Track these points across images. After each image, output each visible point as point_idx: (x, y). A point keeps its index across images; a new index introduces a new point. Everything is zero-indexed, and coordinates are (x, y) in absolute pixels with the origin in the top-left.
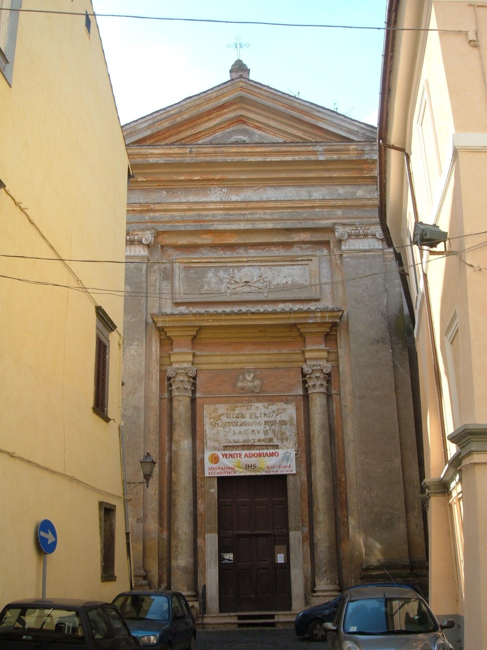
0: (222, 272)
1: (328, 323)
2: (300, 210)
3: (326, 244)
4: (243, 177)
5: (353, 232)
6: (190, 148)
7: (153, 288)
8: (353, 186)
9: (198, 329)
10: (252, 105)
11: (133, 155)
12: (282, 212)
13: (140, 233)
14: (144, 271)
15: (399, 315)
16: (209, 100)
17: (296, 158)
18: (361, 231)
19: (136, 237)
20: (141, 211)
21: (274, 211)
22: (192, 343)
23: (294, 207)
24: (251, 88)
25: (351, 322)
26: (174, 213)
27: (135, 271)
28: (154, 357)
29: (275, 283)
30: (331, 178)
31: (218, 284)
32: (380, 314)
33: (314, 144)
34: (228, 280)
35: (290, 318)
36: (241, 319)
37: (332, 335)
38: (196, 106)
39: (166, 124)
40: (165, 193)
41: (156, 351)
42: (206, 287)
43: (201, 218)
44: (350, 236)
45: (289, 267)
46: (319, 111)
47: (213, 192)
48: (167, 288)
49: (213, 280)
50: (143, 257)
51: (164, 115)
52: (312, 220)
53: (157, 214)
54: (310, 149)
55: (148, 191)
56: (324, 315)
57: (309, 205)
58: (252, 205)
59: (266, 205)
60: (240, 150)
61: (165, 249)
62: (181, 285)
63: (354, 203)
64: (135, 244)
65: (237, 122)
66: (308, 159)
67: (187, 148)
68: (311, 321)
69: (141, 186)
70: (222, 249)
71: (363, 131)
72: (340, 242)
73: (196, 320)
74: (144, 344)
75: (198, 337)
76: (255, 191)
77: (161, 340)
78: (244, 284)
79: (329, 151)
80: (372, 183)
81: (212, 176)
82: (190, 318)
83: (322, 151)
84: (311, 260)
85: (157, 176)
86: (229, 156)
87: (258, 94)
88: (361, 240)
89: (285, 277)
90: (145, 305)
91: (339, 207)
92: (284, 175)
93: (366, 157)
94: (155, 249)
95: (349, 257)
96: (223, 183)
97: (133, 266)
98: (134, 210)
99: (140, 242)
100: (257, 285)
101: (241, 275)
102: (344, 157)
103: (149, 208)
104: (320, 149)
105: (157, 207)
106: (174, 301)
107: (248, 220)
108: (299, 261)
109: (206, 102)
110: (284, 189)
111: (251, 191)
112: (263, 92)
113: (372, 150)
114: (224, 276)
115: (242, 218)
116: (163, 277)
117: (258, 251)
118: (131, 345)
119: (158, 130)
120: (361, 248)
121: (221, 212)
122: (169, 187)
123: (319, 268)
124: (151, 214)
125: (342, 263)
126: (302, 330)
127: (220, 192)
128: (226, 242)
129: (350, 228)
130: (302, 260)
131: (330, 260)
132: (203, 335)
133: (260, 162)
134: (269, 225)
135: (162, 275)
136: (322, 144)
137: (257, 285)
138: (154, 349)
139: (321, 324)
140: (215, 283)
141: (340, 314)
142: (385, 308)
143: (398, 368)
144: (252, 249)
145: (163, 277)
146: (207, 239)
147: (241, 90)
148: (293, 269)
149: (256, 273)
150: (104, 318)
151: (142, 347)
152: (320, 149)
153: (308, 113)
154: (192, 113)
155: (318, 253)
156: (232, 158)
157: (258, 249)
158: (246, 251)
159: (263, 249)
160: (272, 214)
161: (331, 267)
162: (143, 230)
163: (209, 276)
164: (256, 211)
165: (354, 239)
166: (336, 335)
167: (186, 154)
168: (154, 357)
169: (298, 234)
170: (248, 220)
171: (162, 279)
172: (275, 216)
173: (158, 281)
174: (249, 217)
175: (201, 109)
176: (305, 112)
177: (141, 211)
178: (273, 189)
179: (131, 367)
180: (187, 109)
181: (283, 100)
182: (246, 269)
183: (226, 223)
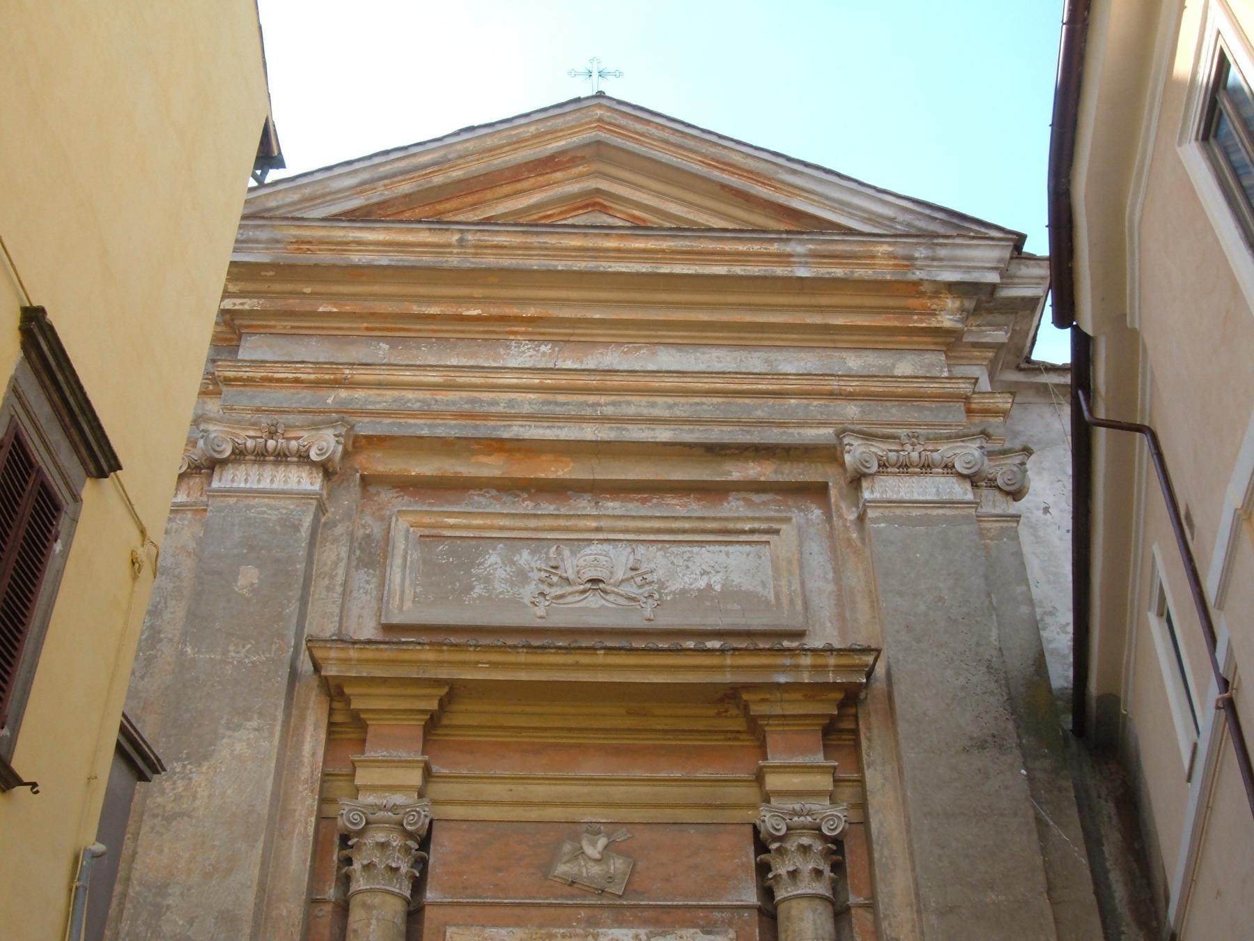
0: (525, 554)
1: (834, 686)
2: (747, 401)
3: (818, 492)
4: (597, 316)
5: (893, 456)
6: (462, 231)
7: (327, 581)
8: (883, 354)
9: (444, 691)
10: (621, 166)
11: (310, 243)
12: (697, 404)
13: (305, 434)
14: (304, 532)
15: (1036, 678)
16: (518, 143)
17: (738, 270)
18: (915, 455)
19: (294, 444)
20: (317, 384)
21: (677, 400)
22: (426, 741)
23: (731, 391)
24: (623, 122)
25: (901, 689)
26: (404, 393)
27: (278, 528)
28: (305, 772)
29: (675, 586)
30: (827, 328)
31: (512, 584)
32: (984, 669)
33: (784, 236)
34: (543, 574)
35: (721, 668)
36: (577, 666)
37: (842, 731)
38: (484, 151)
39: (406, 188)
40: (387, 347)
41: (314, 754)
42: (479, 590)
43: (478, 409)
44: (883, 465)
45: (717, 548)
46: (794, 172)
47: (514, 350)
48: (368, 587)
49: (501, 573)
50: (305, 495)
51: (401, 165)
52: (780, 425)
53: (359, 394)
54: (774, 248)
55: (343, 339)
56: (820, 661)
57: (770, 387)
58: (615, 381)
59: (655, 383)
60: (590, 243)
61: (372, 490)
62: (407, 583)
63: (891, 387)
64: (288, 463)
65: (586, 206)
66: (767, 274)
67: (452, 231)
68: (782, 679)
69: (323, 328)
70: (531, 497)
71: (908, 218)
72: (857, 480)
73: (441, 663)
74: (278, 728)
75: (445, 722)
76: (625, 353)
77: (331, 724)
78: (589, 585)
79: (824, 257)
80: (933, 347)
81: (514, 311)
82: (423, 656)
83: (805, 256)
84: (777, 532)
85: (367, 304)
86: (561, 257)
87: (642, 135)
88: (915, 479)
89: (704, 573)
90: (294, 620)
91: (850, 396)
92: (703, 316)
93: (919, 275)
94: (345, 484)
95: (884, 519)
96: (542, 330)
97: (274, 518)
98: (297, 381)
99: (303, 458)
100: (623, 589)
101: (581, 563)
102: (860, 273)
103: (338, 376)
104: (800, 249)
105: (361, 375)
106: (383, 621)
107: (605, 419)
108: (743, 532)
109: (508, 144)
110: (703, 353)
111: (616, 355)
112: (652, 130)
113: (933, 259)
114: (533, 565)
115: (589, 412)
116: (359, 559)
117: (630, 506)
118: (238, 727)
119: (383, 198)
120: (916, 497)
121: (532, 396)
122: (397, 334)
123: (801, 553)
124: (343, 394)
125: (863, 540)
126: (756, 709)
127: (532, 352)
128: (543, 476)
129: (885, 446)
130: (752, 531)
131: (831, 535)
132: (464, 715)
133: (643, 274)
134: (664, 434)
135: (358, 553)
136: (805, 237)
137: (623, 589)
138: (307, 748)
139: (814, 690)
140: (506, 581)
141: (869, 659)
142: (995, 653)
143: (1048, 825)
144: (613, 500)
145: (359, 559)
146: (491, 467)
147: (600, 128)
148: (727, 554)
149: (623, 559)
150: (60, 377)
151: (272, 734)
152: (800, 249)
153: (766, 177)
154: (473, 168)
155: (797, 517)
156: (569, 263)
157: (632, 500)
158: (597, 503)
159: (644, 501)
160: (670, 407)
161: (833, 549)
162: (315, 426)
163: (489, 562)
164: (629, 398)
165: (895, 474)
166: (855, 732)
167: (450, 245)
168: (305, 772)
169: (740, 464)
170: (605, 419)
171: (354, 563)
172: (678, 412)
173: (343, 564)
174: (609, 411)
175: (496, 162)
176: (758, 174)
177: (317, 384)
178: (673, 351)
179: (229, 792)
180: (461, 157)
181: (705, 149)
182: (595, 548)
183: (546, 424)
